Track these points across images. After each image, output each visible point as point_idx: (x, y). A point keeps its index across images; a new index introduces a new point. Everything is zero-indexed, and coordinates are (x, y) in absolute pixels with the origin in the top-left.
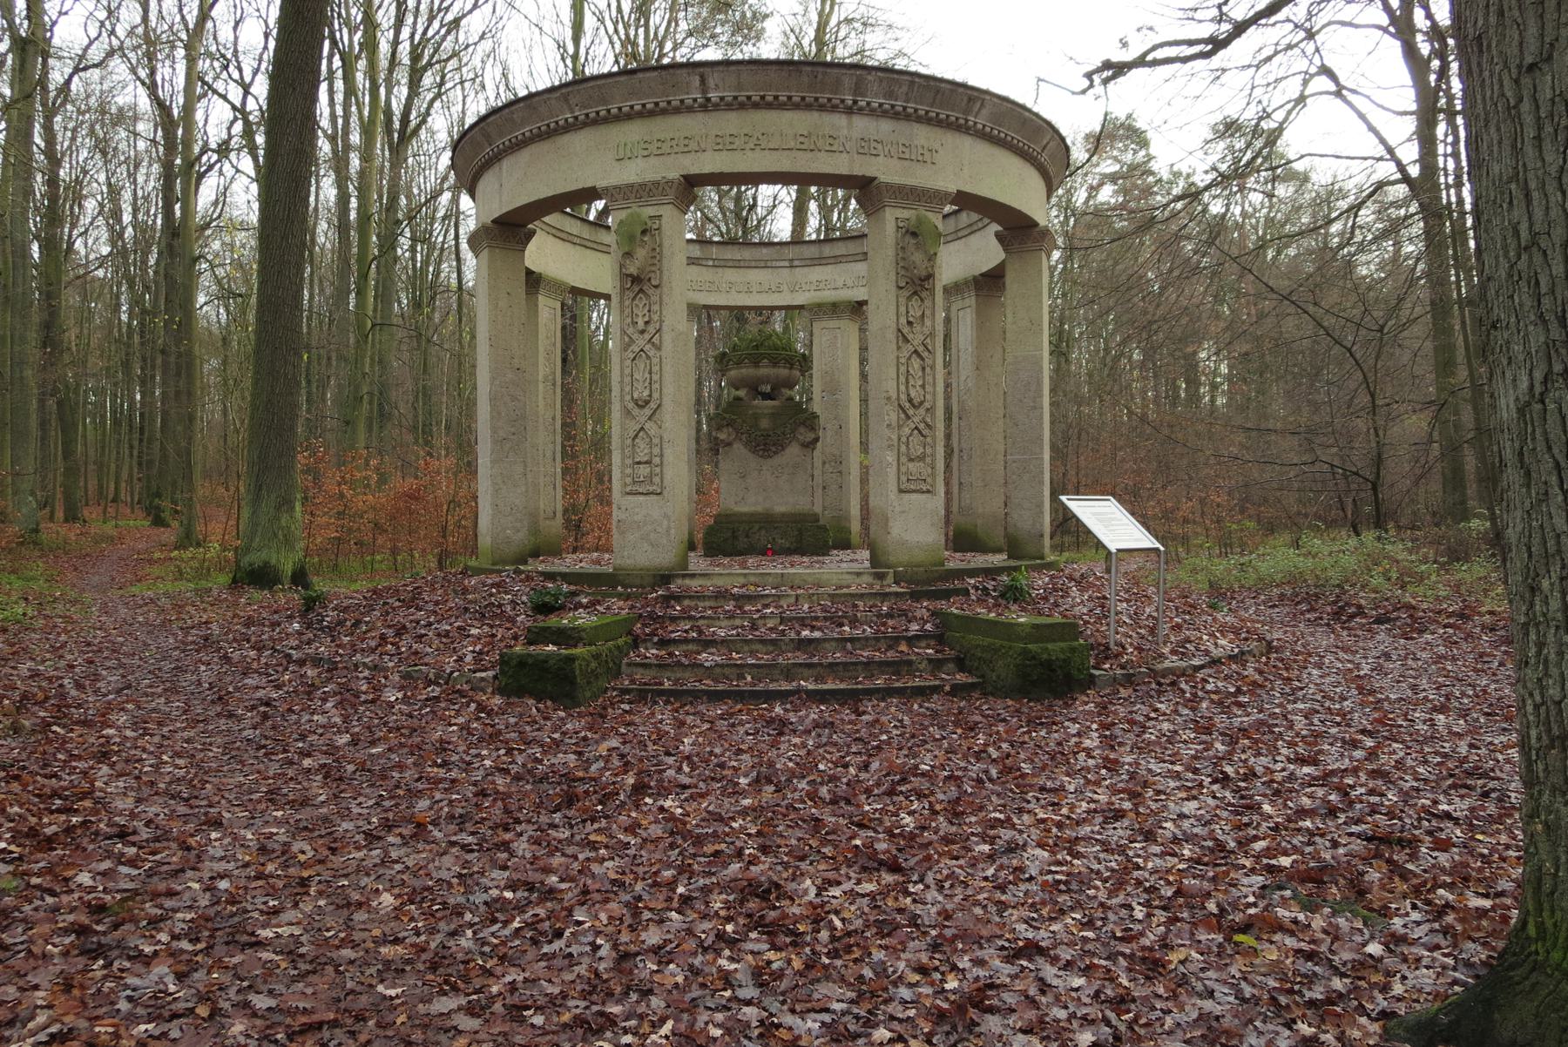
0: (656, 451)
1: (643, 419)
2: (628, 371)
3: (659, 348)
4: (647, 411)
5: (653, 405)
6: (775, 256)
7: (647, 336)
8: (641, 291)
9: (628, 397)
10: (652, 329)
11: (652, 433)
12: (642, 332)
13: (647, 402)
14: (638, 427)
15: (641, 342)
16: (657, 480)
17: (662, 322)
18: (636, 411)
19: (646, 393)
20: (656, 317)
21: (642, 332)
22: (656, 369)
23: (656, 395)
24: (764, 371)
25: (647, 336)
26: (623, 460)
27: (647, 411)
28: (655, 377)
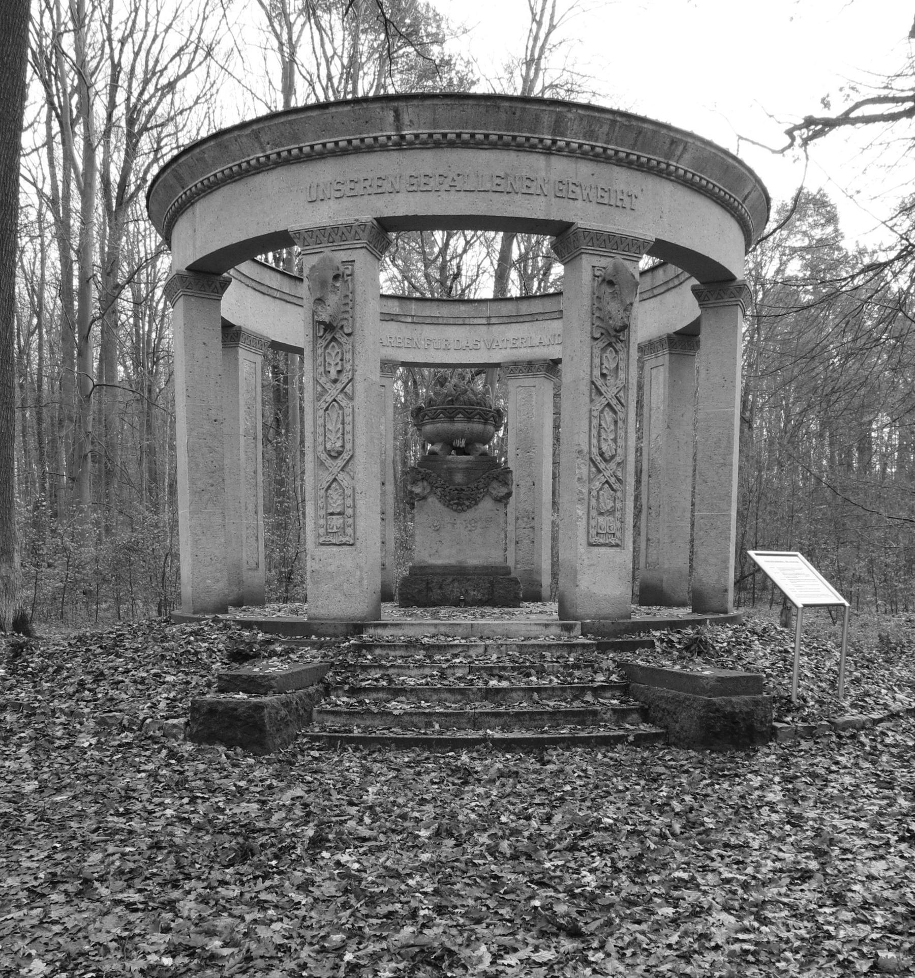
0: (349, 502)
1: (335, 470)
2: (320, 421)
3: (351, 398)
4: (340, 462)
5: (346, 456)
6: (472, 314)
7: (339, 386)
8: (334, 339)
9: (321, 448)
10: (344, 379)
11: (345, 484)
12: (335, 381)
13: (340, 453)
14: (331, 478)
15: (333, 391)
16: (349, 531)
17: (354, 371)
18: (329, 462)
19: (339, 444)
20: (348, 366)
21: (335, 381)
22: (348, 419)
23: (348, 446)
24: (460, 426)
25: (339, 386)
26: (316, 510)
27: (340, 462)
28: (348, 428)
